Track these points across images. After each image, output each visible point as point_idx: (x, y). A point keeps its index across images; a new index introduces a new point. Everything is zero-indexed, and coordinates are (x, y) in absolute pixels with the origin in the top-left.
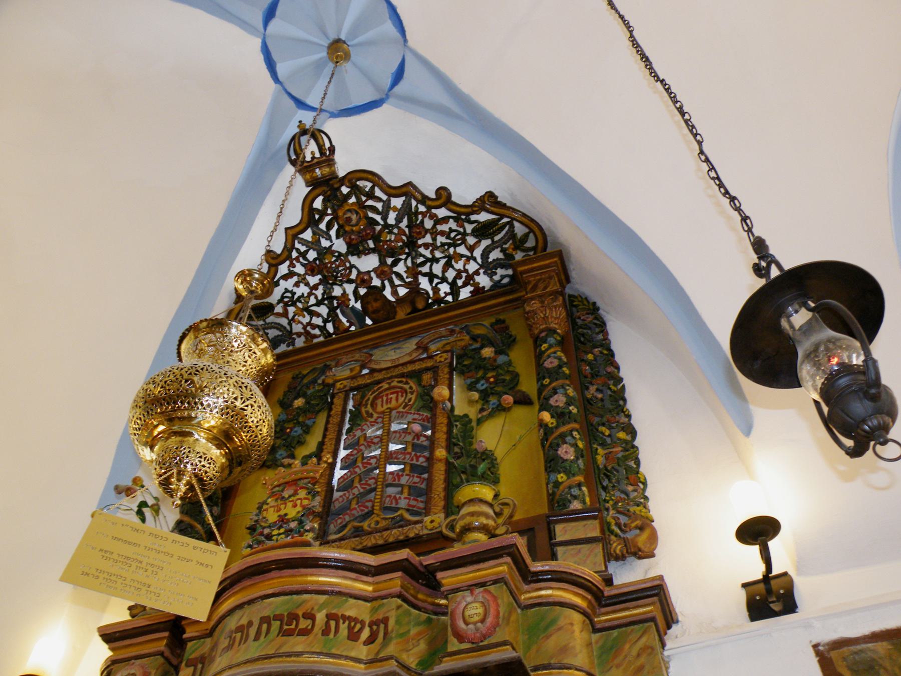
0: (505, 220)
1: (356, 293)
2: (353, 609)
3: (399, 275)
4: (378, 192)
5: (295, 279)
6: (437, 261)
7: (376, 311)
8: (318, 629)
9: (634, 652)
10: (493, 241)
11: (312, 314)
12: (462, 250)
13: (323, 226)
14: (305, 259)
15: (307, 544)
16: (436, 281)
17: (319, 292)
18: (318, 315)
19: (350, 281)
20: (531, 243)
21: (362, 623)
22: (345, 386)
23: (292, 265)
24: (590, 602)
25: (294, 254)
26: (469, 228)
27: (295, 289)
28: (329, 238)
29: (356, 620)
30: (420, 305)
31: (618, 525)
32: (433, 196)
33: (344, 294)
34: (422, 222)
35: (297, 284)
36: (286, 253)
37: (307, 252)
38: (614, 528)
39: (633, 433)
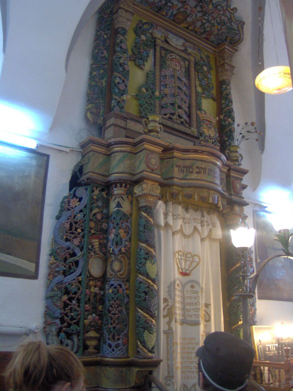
3: (196, 16)
7: (178, 18)
16: (203, 27)
26: (228, 24)
30: (190, 28)
32: (232, 7)
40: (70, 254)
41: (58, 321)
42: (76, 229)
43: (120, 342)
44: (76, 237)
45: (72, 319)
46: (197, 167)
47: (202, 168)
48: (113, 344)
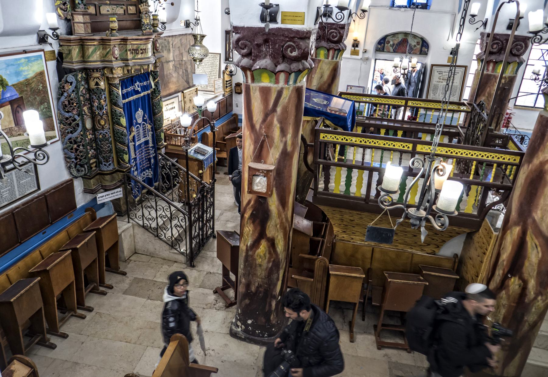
40: (72, 120)
41: (74, 160)
42: (73, 104)
43: (111, 162)
44: (74, 109)
45: (82, 156)
46: (141, 50)
47: (144, 49)
48: (107, 164)
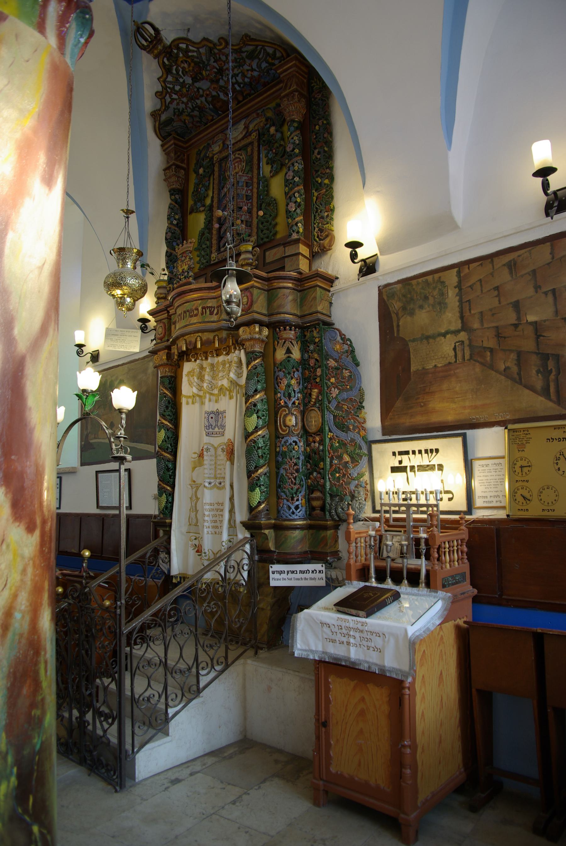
0: (259, 48)
1: (206, 100)
2: (210, 303)
4: (191, 48)
5: (175, 102)
6: (238, 75)
8: (200, 314)
9: (310, 300)
10: (259, 59)
11: (192, 117)
12: (246, 67)
13: (174, 72)
14: (175, 90)
15: (190, 283)
16: (242, 86)
17: (190, 105)
18: (196, 116)
19: (202, 96)
20: (278, 55)
21: (214, 307)
22: (217, 159)
23: (170, 96)
24: (293, 283)
25: (169, 90)
26: (244, 55)
27: (179, 107)
28: (181, 77)
29: (212, 307)
31: (318, 237)
33: (201, 102)
34: (220, 58)
35: (178, 104)
36: (165, 91)
37: (174, 87)
38: (316, 238)
39: (331, 178)
